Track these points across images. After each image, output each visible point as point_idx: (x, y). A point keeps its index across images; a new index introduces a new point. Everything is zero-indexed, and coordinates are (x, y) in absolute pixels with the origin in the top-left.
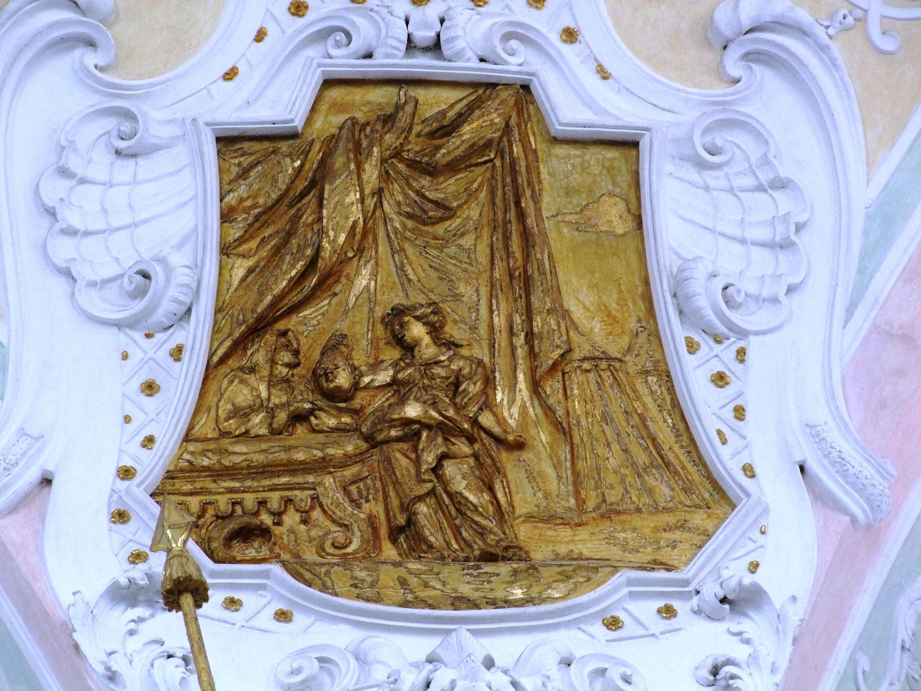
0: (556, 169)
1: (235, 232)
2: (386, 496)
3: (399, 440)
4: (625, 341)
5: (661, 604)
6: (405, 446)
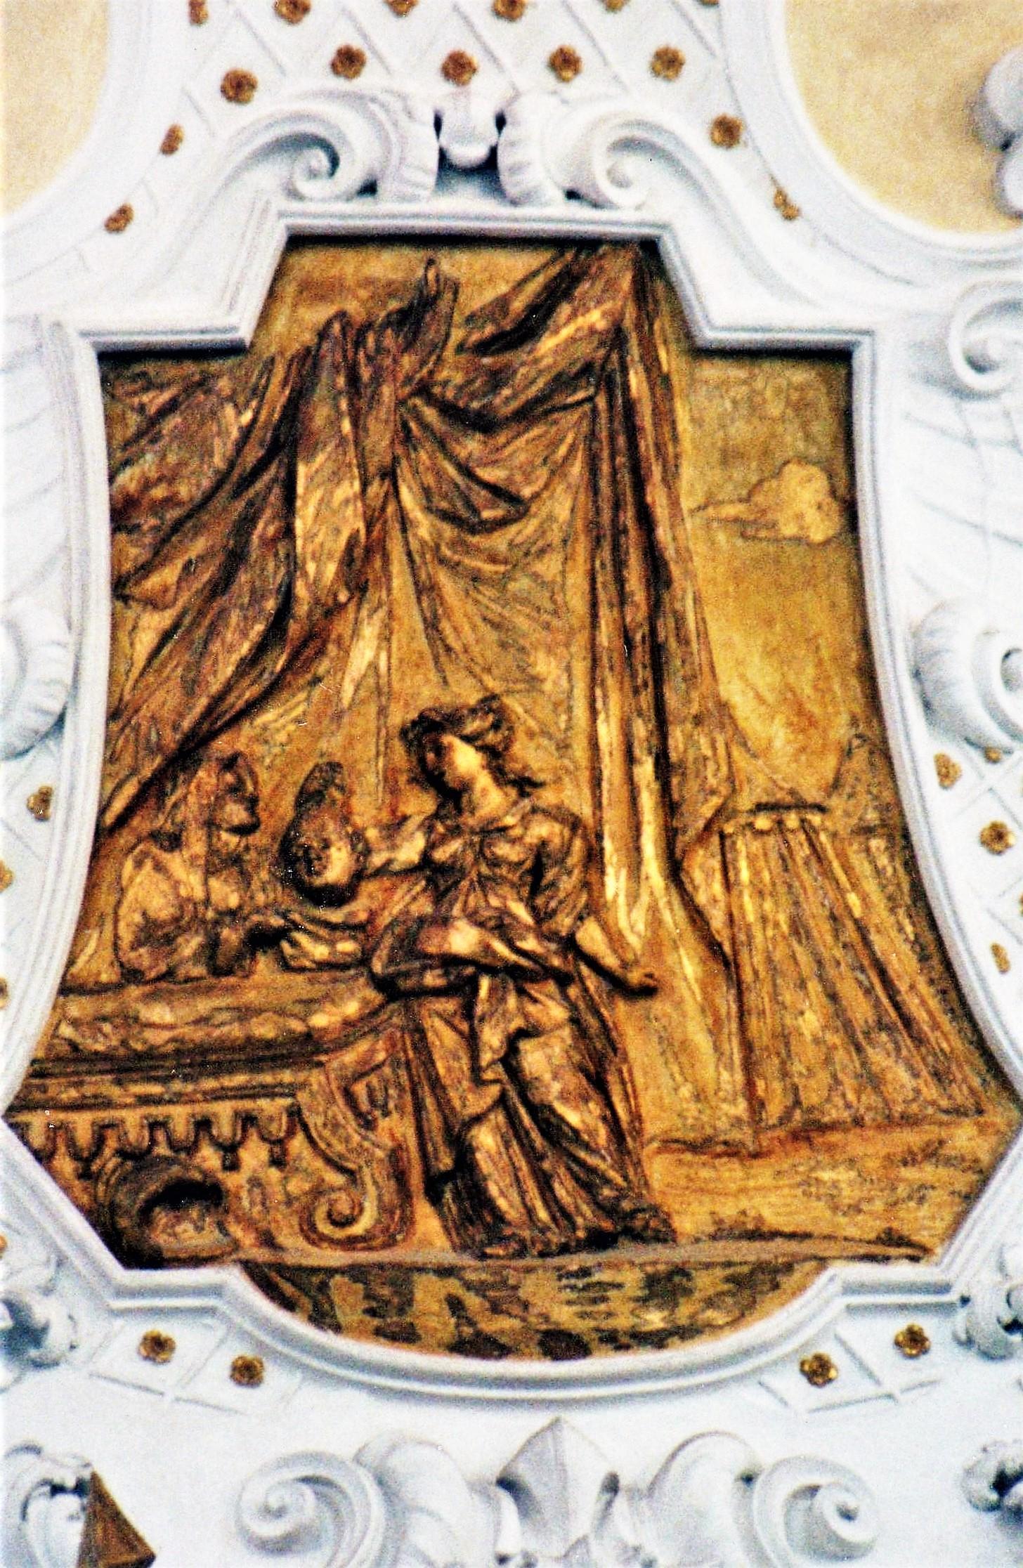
0: (705, 411)
1: (135, 553)
2: (419, 1108)
3: (437, 992)
4: (829, 764)
5: (899, 1324)
6: (449, 1005)
